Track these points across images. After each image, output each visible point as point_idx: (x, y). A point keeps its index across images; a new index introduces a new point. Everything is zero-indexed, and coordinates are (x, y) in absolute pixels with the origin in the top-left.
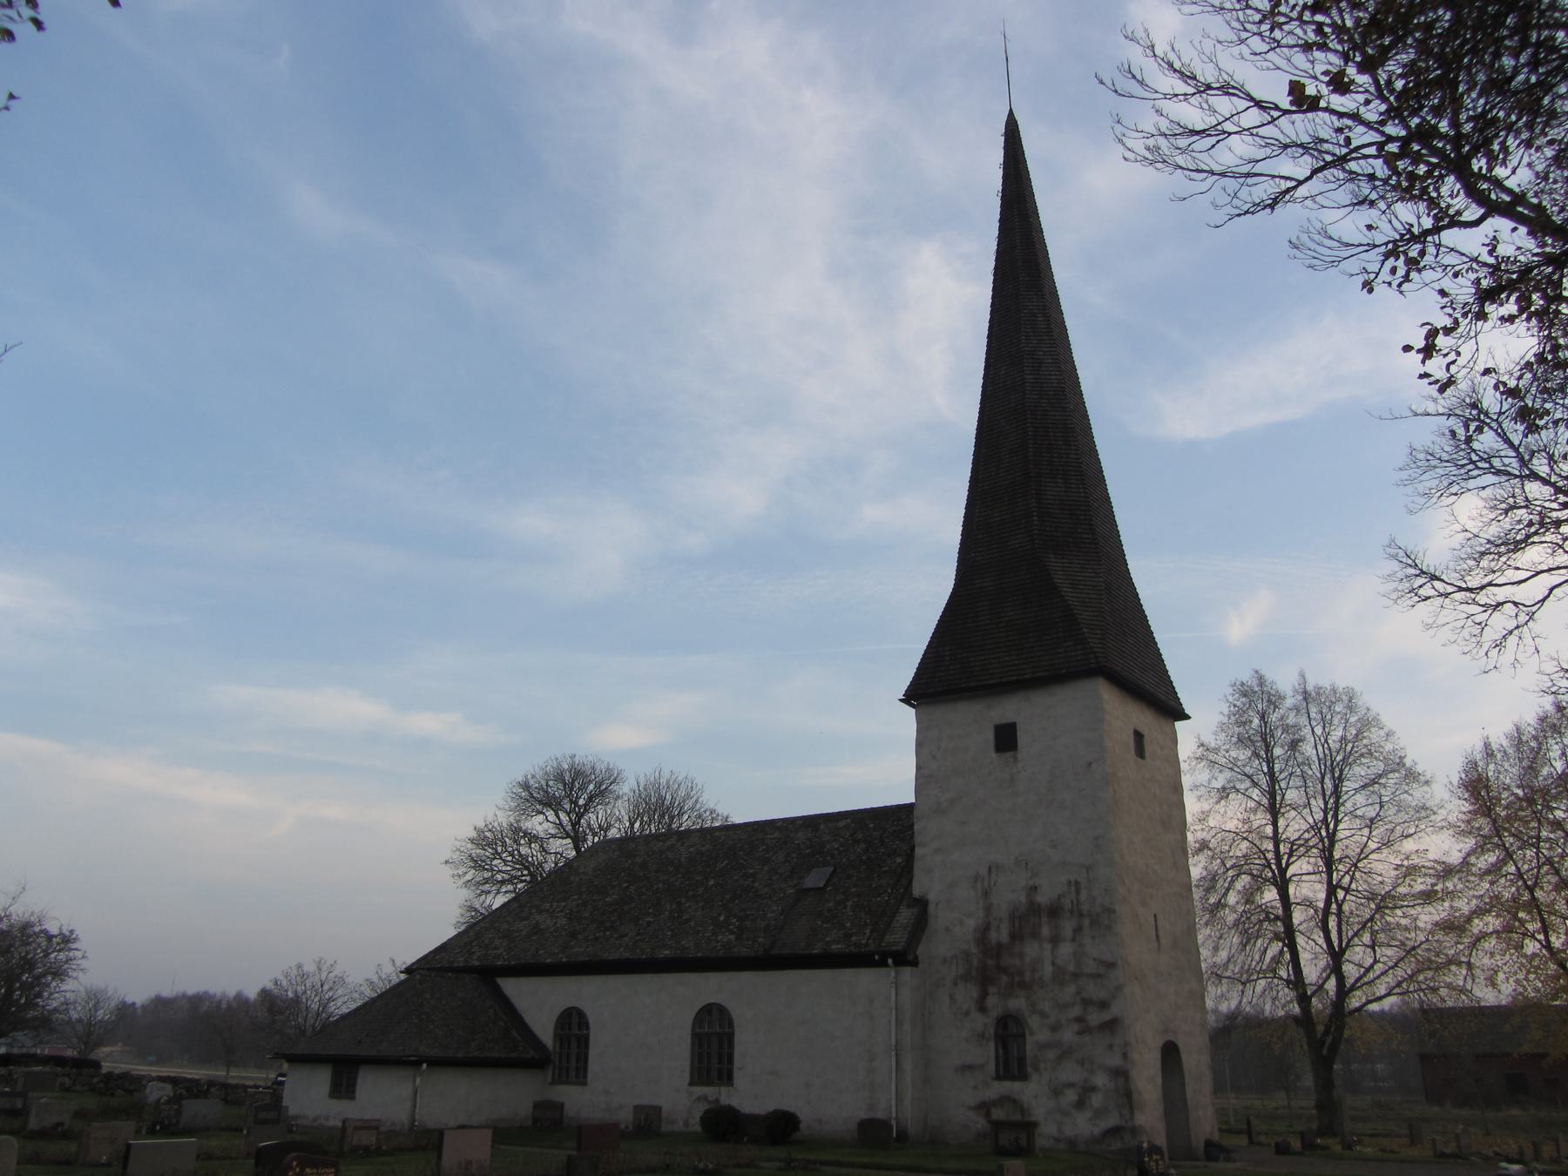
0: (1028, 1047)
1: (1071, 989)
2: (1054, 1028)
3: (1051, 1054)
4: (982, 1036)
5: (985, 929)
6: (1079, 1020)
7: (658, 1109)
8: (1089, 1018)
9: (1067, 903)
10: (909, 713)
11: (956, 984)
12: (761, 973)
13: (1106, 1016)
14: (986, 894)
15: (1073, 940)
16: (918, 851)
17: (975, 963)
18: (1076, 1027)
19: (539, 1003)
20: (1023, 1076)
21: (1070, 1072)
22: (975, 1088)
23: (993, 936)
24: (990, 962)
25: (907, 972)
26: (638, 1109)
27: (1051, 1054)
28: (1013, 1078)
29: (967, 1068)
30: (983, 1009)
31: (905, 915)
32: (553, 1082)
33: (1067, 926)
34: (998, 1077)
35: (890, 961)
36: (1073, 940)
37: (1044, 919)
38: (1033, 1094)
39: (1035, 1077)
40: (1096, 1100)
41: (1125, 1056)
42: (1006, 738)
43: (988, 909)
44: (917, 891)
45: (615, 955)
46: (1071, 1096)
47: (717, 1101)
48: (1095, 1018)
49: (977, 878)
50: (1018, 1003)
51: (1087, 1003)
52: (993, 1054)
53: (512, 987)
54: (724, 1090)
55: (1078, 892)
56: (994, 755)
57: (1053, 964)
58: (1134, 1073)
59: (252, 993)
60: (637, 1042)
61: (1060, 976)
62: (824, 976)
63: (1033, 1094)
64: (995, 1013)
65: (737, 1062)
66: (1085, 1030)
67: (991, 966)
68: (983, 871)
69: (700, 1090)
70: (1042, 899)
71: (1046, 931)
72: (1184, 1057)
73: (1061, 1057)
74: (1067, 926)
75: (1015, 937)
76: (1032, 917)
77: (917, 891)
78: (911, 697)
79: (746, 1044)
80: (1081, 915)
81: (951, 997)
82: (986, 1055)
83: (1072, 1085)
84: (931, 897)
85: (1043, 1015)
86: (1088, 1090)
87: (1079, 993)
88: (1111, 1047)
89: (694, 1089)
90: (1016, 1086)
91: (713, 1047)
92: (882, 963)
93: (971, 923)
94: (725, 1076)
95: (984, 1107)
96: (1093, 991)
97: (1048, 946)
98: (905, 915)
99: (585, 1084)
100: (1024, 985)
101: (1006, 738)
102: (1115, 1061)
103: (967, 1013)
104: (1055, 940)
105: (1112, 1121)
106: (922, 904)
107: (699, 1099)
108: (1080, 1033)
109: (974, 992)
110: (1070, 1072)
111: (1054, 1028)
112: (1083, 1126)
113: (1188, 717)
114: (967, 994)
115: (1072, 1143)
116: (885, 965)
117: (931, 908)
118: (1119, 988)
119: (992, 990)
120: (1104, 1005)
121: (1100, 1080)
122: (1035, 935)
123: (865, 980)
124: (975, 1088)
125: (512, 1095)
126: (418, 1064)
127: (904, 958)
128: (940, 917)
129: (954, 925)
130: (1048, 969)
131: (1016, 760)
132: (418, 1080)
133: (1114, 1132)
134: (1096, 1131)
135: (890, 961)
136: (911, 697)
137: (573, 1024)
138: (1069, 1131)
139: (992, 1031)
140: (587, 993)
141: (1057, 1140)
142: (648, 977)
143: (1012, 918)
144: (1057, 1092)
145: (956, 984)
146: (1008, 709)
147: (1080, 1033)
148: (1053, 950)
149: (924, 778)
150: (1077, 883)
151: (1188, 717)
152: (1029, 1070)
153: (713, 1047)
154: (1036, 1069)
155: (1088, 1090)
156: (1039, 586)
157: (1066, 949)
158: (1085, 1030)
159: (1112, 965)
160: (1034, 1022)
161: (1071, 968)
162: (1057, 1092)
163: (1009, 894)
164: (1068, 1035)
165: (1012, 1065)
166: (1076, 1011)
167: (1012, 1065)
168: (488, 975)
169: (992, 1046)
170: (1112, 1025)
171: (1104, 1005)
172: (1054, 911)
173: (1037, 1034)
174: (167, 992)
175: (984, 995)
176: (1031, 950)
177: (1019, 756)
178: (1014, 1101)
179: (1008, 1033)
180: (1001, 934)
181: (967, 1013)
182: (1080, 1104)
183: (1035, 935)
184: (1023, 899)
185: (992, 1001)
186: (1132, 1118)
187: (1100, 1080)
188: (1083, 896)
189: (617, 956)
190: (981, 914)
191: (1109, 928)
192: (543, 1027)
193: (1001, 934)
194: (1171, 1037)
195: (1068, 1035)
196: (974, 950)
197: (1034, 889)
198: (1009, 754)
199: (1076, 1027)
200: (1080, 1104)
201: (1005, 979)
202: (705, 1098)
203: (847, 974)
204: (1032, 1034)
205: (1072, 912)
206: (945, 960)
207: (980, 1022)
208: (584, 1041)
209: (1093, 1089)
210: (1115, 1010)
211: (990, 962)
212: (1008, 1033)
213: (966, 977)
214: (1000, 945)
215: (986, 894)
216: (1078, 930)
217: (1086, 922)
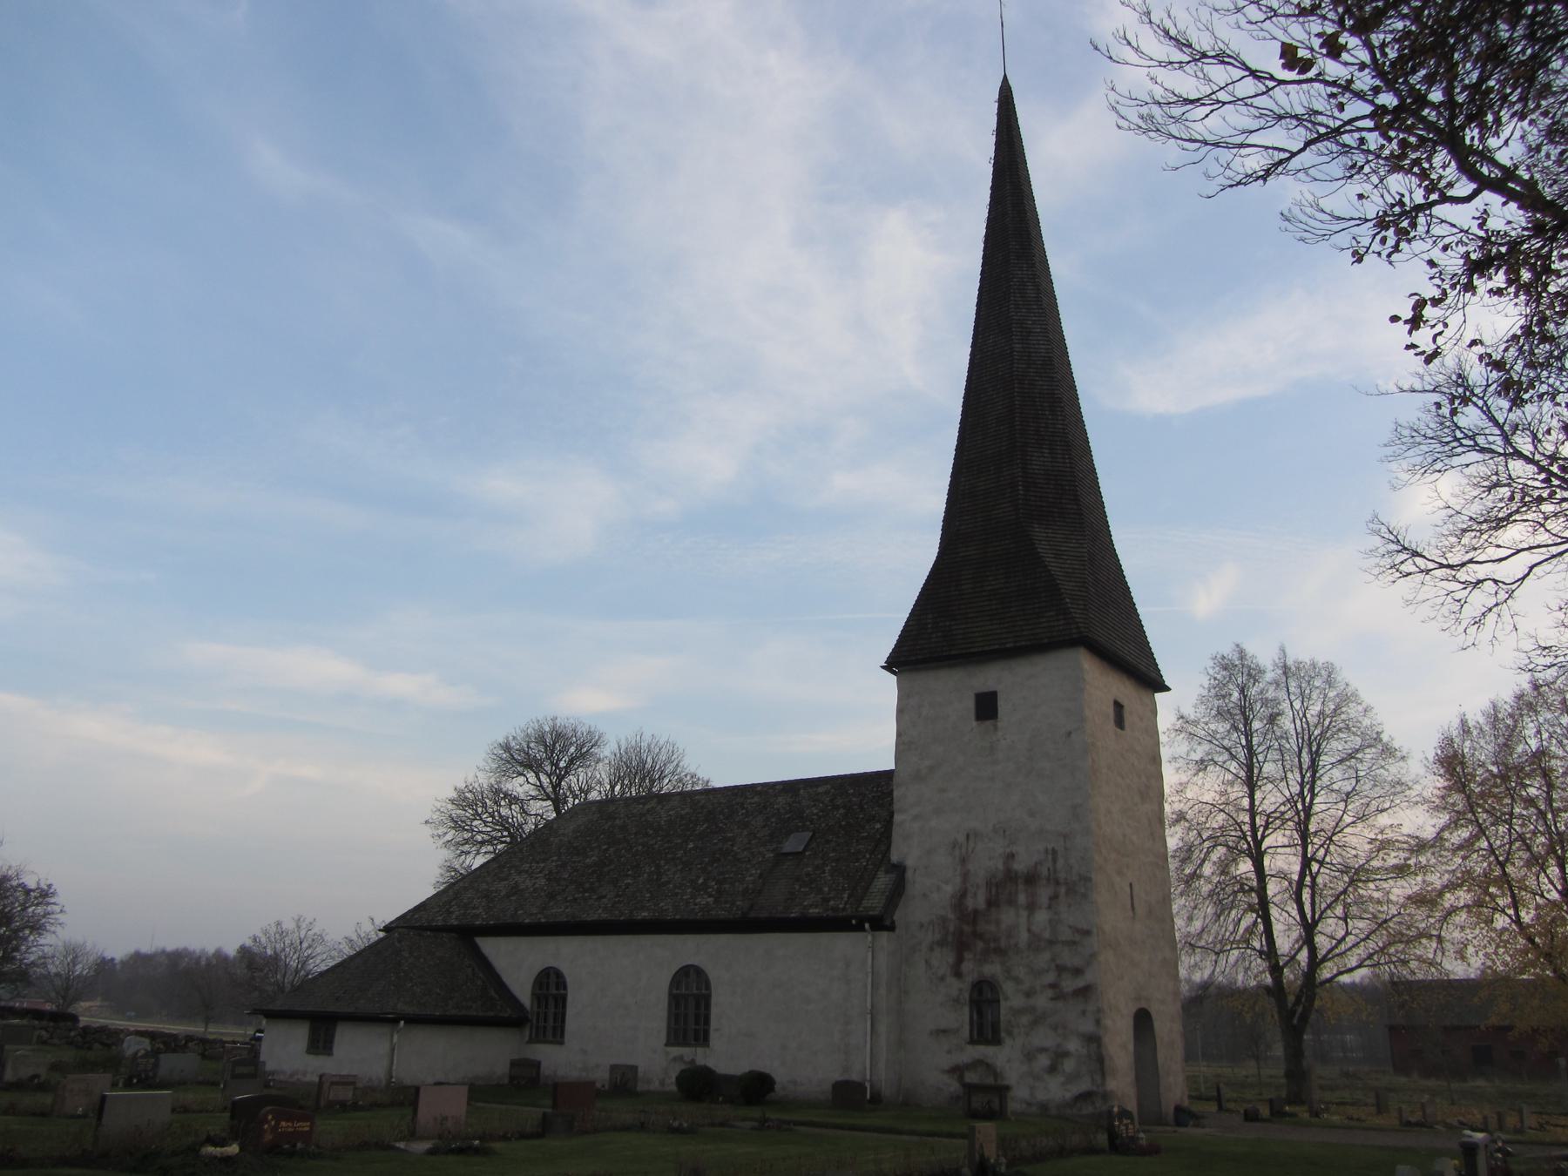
1: (1046, 956)
2: (1028, 994)
3: (1025, 1020)
4: (957, 1001)
5: (962, 895)
6: (1053, 986)
7: (634, 1069)
8: (1063, 984)
9: (1044, 871)
10: (891, 680)
11: (931, 949)
13: (1080, 983)
14: (963, 861)
15: (1049, 907)
16: (897, 818)
17: (951, 929)
18: (1050, 993)
19: (517, 963)
20: (996, 1040)
21: (1043, 1037)
22: (949, 1052)
23: (970, 903)
24: (967, 929)
25: (884, 936)
26: (614, 1068)
27: (1025, 1020)
28: (988, 1042)
30: (958, 974)
31: (883, 881)
32: (531, 1041)
33: (1044, 893)
34: (972, 1042)
35: (867, 926)
37: (1021, 887)
38: (1006, 1058)
39: (1008, 1042)
40: (1069, 1065)
41: (1098, 1022)
42: (986, 707)
43: (965, 876)
44: (894, 858)
45: (593, 916)
46: (1044, 1061)
47: (693, 1061)
48: (1069, 984)
49: (954, 845)
50: (993, 969)
51: (1061, 969)
53: (488, 945)
54: (700, 1050)
55: (1055, 861)
56: (974, 723)
57: (1029, 930)
58: (1106, 1040)
59: (231, 950)
60: (614, 1000)
61: (1036, 944)
63: (1006, 1058)
64: (970, 979)
65: (713, 1023)
66: (1059, 996)
67: (967, 932)
68: (961, 838)
69: (676, 1051)
70: (1020, 866)
71: (1022, 898)
72: (1157, 1024)
73: (1035, 1023)
75: (992, 903)
76: (1010, 884)
77: (894, 858)
78: (890, 666)
80: (1057, 883)
82: (961, 1019)
83: (1043, 1050)
84: (910, 863)
85: (1017, 980)
86: (1060, 1055)
87: (1053, 960)
88: (1084, 1013)
89: (669, 1049)
91: (690, 1009)
92: (859, 928)
93: (949, 889)
94: (701, 1037)
95: (957, 1071)
96: (1068, 958)
97: (1024, 913)
98: (883, 881)
99: (562, 1043)
100: (1001, 952)
101: (986, 707)
102: (1087, 1026)
103: (942, 979)
104: (1032, 907)
105: (1084, 1085)
106: (899, 870)
107: (675, 1059)
109: (951, 959)
110: (1043, 1037)
111: (1028, 994)
112: (1055, 1091)
113: (1168, 689)
114: (943, 960)
115: (1044, 1107)
116: (863, 930)
117: (909, 874)
118: (1093, 956)
119: (968, 955)
120: (1078, 972)
121: (1073, 1045)
122: (1012, 902)
123: (843, 944)
124: (949, 1052)
125: (490, 1054)
126: (395, 1021)
127: (881, 923)
128: (917, 883)
130: (1024, 936)
131: (996, 728)
132: (396, 1037)
133: (1086, 1096)
134: (1068, 1095)
135: (867, 926)
136: (890, 666)
137: (551, 985)
138: (1041, 1096)
139: (967, 995)
140: (565, 953)
141: (1029, 1104)
143: (989, 884)
144: (1029, 1056)
145: (931, 949)
146: (989, 677)
149: (904, 745)
150: (1054, 852)
151: (1168, 689)
152: (1003, 1034)
153: (690, 1009)
154: (1010, 1034)
155: (1060, 1055)
156: (1023, 556)
157: (1042, 917)
158: (1059, 996)
159: (1087, 933)
160: (1008, 987)
161: (1047, 935)
162: (1029, 1056)
163: (987, 861)
164: (1042, 1001)
165: (986, 1030)
166: (1050, 977)
167: (986, 1030)
168: (467, 934)
169: (966, 1010)
170: (1085, 992)
171: (1078, 972)
172: (1031, 879)
173: (1012, 999)
174: (146, 948)
176: (1007, 917)
177: (999, 724)
178: (988, 1065)
179: (983, 998)
180: (978, 901)
181: (942, 979)
182: (1052, 1069)
183: (1012, 902)
184: (1001, 867)
185: (967, 966)
186: (1103, 1084)
187: (1073, 1045)
188: (1060, 863)
189: (595, 917)
190: (958, 880)
191: (1085, 896)
192: (522, 987)
193: (978, 901)
194: (1144, 1005)
195: (1042, 1001)
196: (951, 916)
197: (1012, 856)
198: (988, 723)
199: (1050, 993)
200: (1052, 1069)
201: (980, 945)
202: (680, 1058)
203: (824, 938)
204: (1006, 999)
205: (1048, 880)
206: (922, 926)
207: (955, 987)
208: (561, 1001)
209: (1066, 1054)
210: (1089, 977)
211: (967, 929)
212: (983, 998)
213: (942, 943)
214: (976, 912)
215: (963, 861)
216: (1054, 897)
217: (1063, 890)
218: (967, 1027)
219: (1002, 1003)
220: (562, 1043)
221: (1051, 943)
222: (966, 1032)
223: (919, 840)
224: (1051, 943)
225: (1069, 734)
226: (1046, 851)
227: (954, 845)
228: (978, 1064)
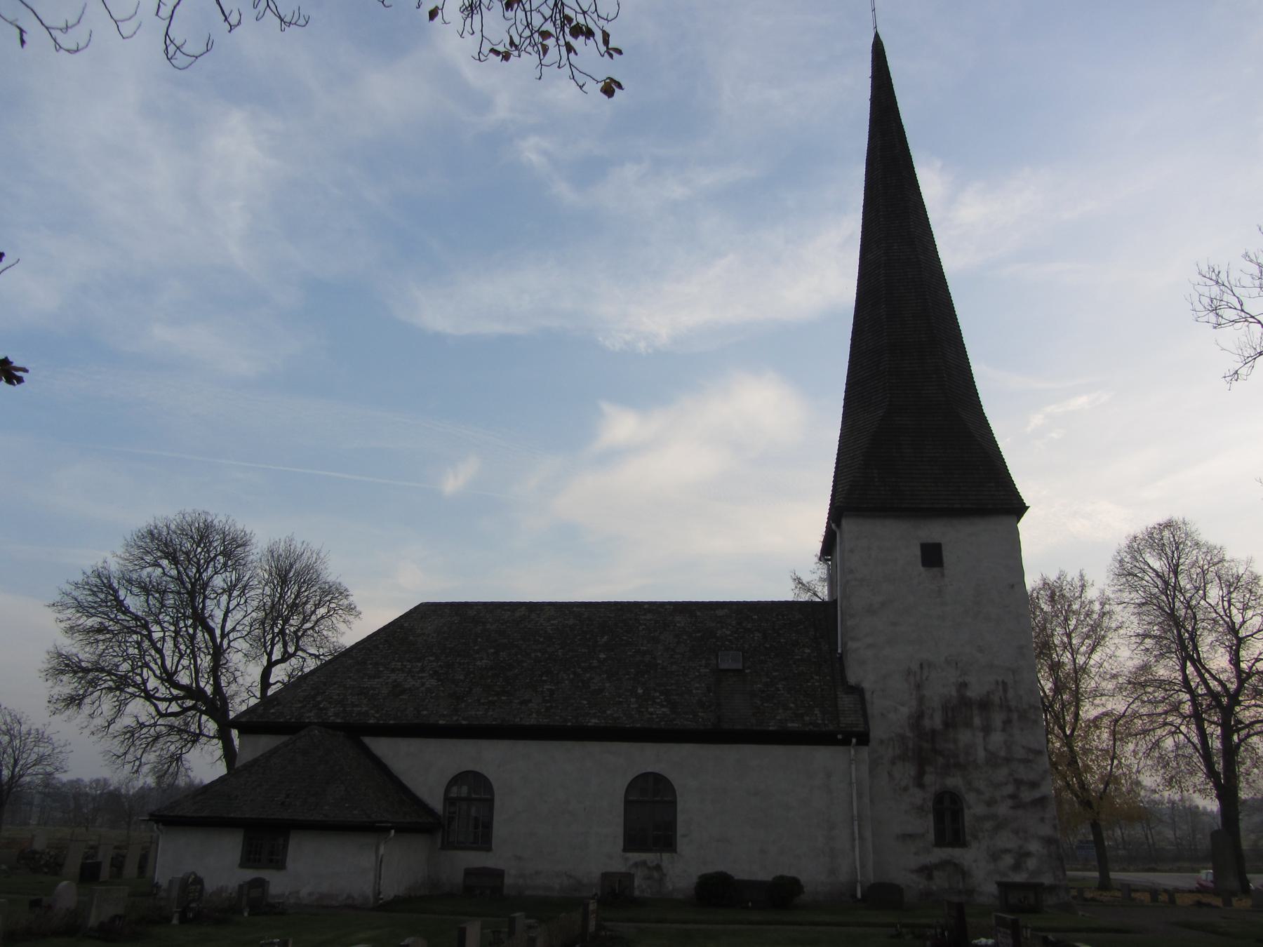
0: (967, 818)
1: (1003, 772)
2: (991, 803)
3: (988, 825)
5: (918, 718)
6: (1013, 796)
12: (706, 746)
14: (919, 687)
17: (911, 745)
18: (1010, 802)
19: (426, 767)
21: (1006, 840)
23: (927, 723)
25: (865, 752)
26: (605, 876)
27: (988, 825)
29: (907, 837)
30: (921, 786)
32: (443, 848)
33: (998, 719)
35: (854, 740)
36: (1004, 730)
38: (972, 857)
42: (932, 556)
43: (921, 700)
45: (532, 720)
46: (1008, 860)
48: (1027, 795)
50: (954, 781)
51: (1019, 783)
52: (932, 824)
53: (382, 747)
54: (666, 856)
55: (1005, 691)
56: (922, 569)
57: (985, 749)
60: (557, 809)
61: (993, 760)
65: (681, 830)
66: (1018, 804)
67: (927, 747)
70: (972, 693)
71: (977, 721)
75: (947, 725)
76: (961, 708)
79: (691, 809)
80: (1009, 710)
81: (890, 775)
83: (1007, 851)
84: (866, 685)
85: (979, 792)
90: (955, 853)
91: (651, 816)
93: (905, 711)
95: (926, 871)
97: (981, 734)
103: (906, 789)
104: (987, 730)
106: (858, 691)
108: (1012, 808)
110: (1006, 840)
114: (905, 772)
117: (868, 696)
120: (1034, 785)
121: (1034, 847)
123: (823, 756)
125: (394, 866)
128: (876, 705)
129: (890, 712)
130: (981, 754)
131: (943, 575)
132: (382, 850)
135: (854, 740)
139: (930, 804)
140: (489, 757)
142: (569, 744)
144: (995, 856)
146: (934, 531)
147: (1012, 808)
148: (984, 738)
152: (968, 838)
153: (651, 816)
155: (1022, 855)
157: (997, 738)
160: (970, 798)
161: (1003, 754)
163: (940, 688)
164: (1003, 809)
166: (1010, 789)
168: (355, 731)
169: (931, 817)
171: (1034, 785)
172: (984, 705)
173: (974, 808)
175: (921, 774)
176: (964, 737)
178: (955, 865)
180: (935, 721)
181: (906, 789)
184: (954, 693)
185: (928, 779)
187: (1034, 847)
188: (1011, 694)
189: (533, 722)
193: (935, 721)
195: (1003, 809)
196: (909, 734)
197: (964, 685)
198: (935, 569)
199: (1010, 802)
201: (941, 760)
203: (802, 751)
204: (969, 808)
206: (882, 742)
209: (1028, 854)
214: (933, 732)
215: (919, 687)
216: (1007, 723)
217: (1015, 716)
218: (932, 832)
219: (966, 811)
220: (489, 849)
221: (1008, 760)
222: (931, 836)
223: (878, 664)
224: (1008, 760)
225: (1013, 586)
226: (997, 682)
227: (909, 672)
228: (943, 865)
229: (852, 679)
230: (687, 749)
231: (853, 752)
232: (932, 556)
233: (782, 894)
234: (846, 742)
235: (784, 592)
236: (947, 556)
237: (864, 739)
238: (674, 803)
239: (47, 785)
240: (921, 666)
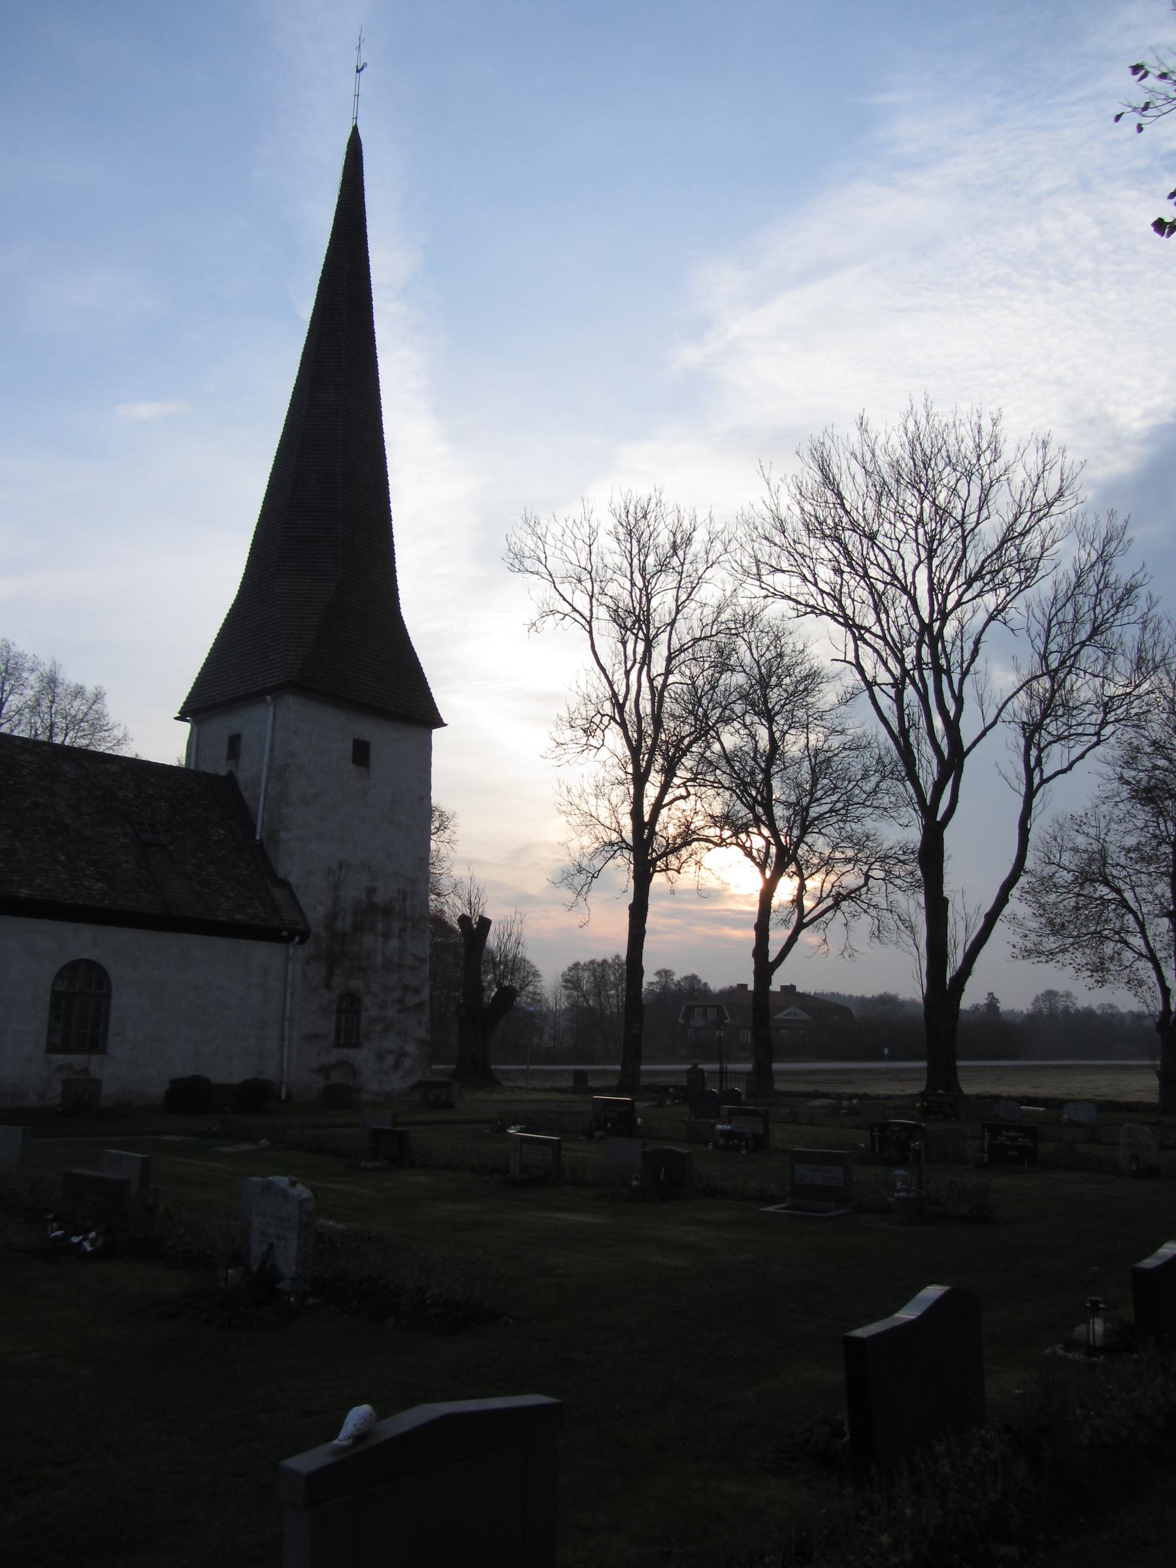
5: (332, 917)
6: (400, 1001)
14: (336, 886)
20: (357, 1045)
28: (348, 1045)
29: (311, 1037)
30: (329, 987)
33: (396, 926)
34: (338, 1045)
36: (399, 937)
38: (363, 1057)
40: (407, 1063)
42: (361, 753)
46: (390, 1060)
47: (86, 1071)
48: (411, 1000)
50: (356, 984)
51: (406, 988)
54: (95, 1058)
55: (405, 899)
56: (352, 766)
57: (383, 954)
62: (222, 944)
63: (363, 1057)
70: (378, 899)
71: (380, 926)
74: (396, 926)
79: (126, 1005)
83: (390, 1052)
84: (292, 880)
86: (402, 1055)
89: (60, 1059)
93: (322, 910)
94: (95, 1043)
95: (325, 1070)
97: (381, 940)
104: (386, 935)
106: (284, 884)
121: (411, 1048)
123: (263, 953)
130: (379, 959)
144: (380, 1057)
150: (405, 893)
155: (402, 1055)
157: (394, 944)
161: (396, 959)
164: (391, 1012)
165: (349, 1036)
167: (349, 1036)
172: (387, 912)
180: (345, 924)
182: (396, 1067)
184: (364, 897)
187: (411, 1048)
193: (345, 924)
195: (391, 1012)
197: (372, 891)
200: (396, 1067)
203: (244, 945)
215: (336, 886)
216: (403, 930)
222: (332, 1037)
226: (399, 890)
229: (281, 873)
230: (128, 934)
231: (291, 951)
232: (361, 753)
233: (255, 1096)
234: (288, 940)
235: (175, 763)
236: (374, 758)
237: (304, 935)
238: (107, 996)
239: (692, 988)
240: (341, 866)
